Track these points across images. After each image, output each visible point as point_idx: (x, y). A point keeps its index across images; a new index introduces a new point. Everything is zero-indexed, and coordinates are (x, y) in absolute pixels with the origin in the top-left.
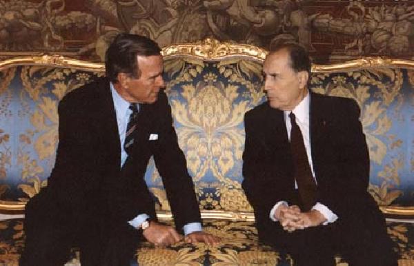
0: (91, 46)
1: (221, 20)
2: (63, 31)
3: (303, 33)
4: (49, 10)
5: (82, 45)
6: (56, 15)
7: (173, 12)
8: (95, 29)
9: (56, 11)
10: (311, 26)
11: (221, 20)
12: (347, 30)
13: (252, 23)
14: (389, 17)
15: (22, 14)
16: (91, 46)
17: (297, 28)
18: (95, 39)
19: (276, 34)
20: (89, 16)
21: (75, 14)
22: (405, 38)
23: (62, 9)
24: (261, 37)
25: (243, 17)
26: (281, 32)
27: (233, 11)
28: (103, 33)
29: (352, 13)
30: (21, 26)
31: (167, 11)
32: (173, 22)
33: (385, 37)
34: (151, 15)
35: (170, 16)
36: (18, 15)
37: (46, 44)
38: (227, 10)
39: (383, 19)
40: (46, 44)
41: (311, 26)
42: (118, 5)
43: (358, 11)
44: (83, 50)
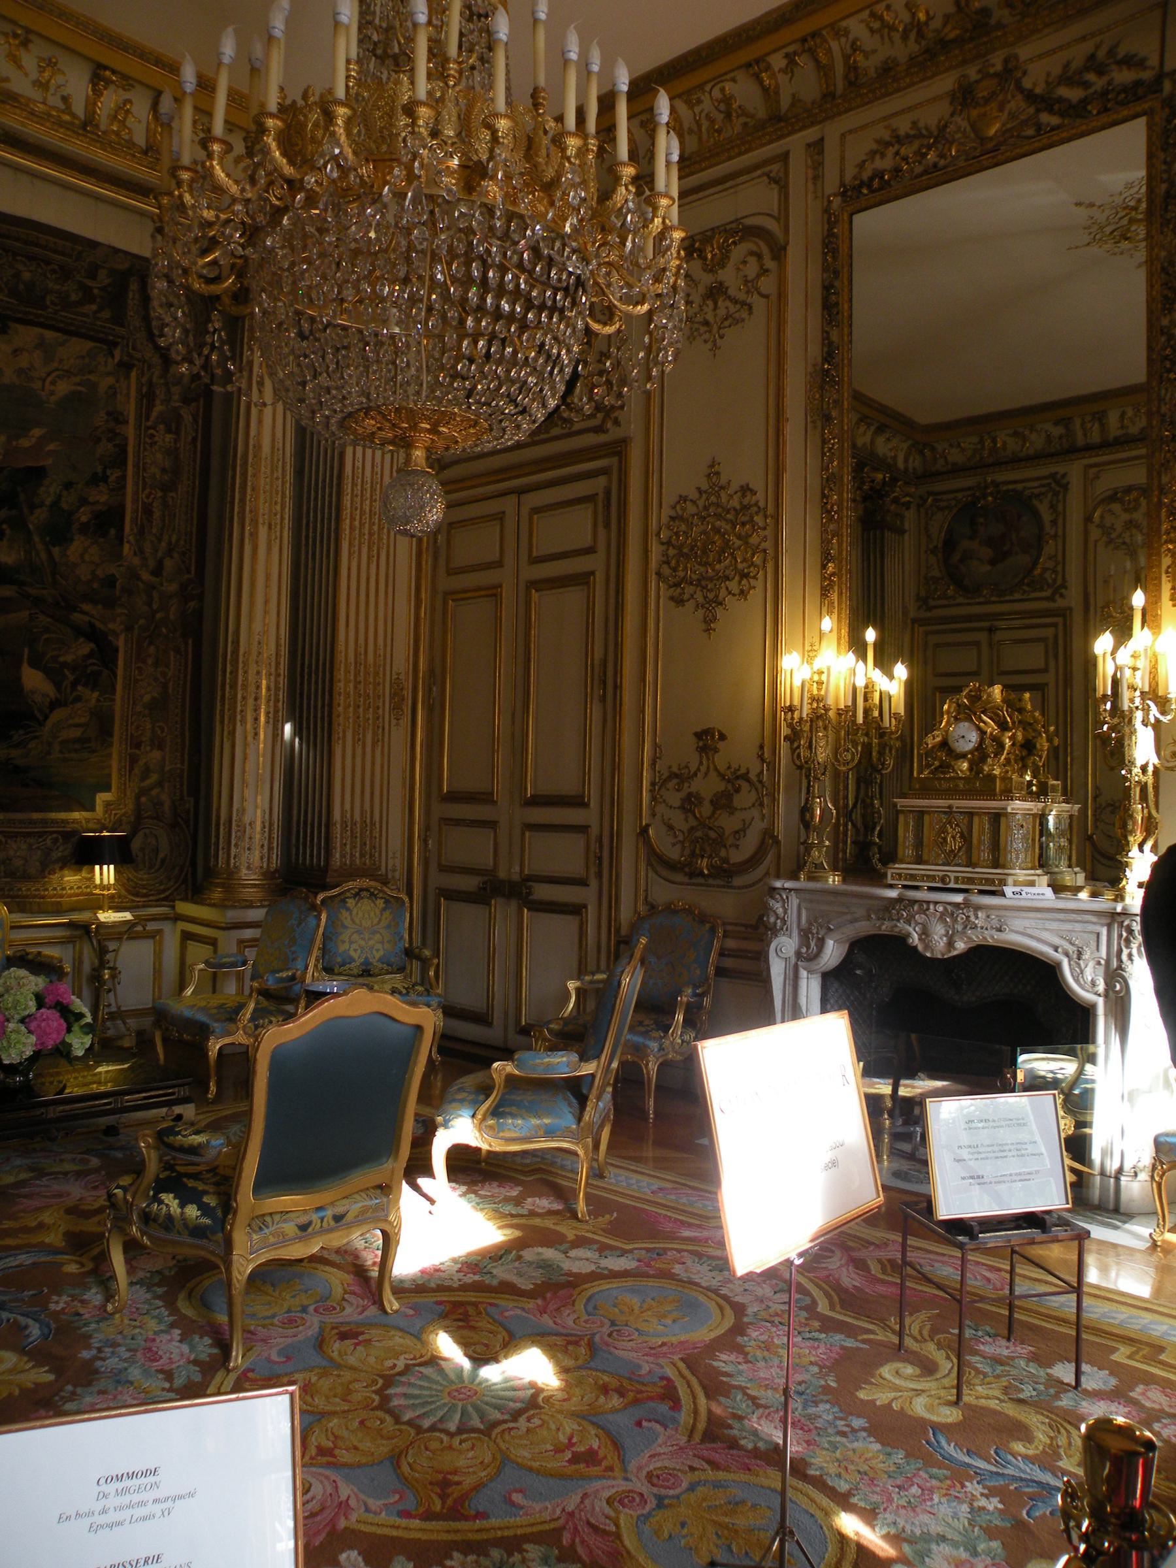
14: (24, 846)
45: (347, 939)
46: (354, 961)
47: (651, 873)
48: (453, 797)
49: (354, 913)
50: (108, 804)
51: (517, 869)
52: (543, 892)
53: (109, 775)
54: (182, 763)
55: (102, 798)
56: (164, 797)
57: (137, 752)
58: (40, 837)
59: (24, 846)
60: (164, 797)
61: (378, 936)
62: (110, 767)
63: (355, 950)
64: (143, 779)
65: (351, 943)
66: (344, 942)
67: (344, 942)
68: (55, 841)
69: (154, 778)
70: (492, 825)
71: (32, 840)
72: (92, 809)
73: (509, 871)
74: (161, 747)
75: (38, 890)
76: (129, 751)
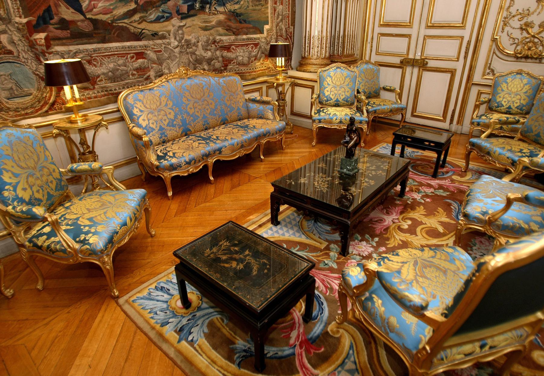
0: (148, 74)
1: (194, 57)
2: (137, 70)
3: (220, 59)
4: (129, 60)
5: (144, 75)
6: (133, 62)
7: (178, 56)
8: (149, 67)
9: (132, 60)
10: (222, 57)
11: (194, 57)
12: (232, 56)
13: (204, 57)
15: (117, 63)
16: (148, 74)
17: (218, 57)
18: (149, 71)
19: (212, 61)
20: (146, 60)
21: (140, 61)
22: (247, 58)
23: (134, 59)
24: (208, 63)
25: (201, 55)
26: (214, 59)
27: (197, 53)
28: (152, 68)
29: (232, 50)
30: (118, 70)
31: (174, 55)
32: (178, 60)
33: (241, 58)
34: (169, 58)
35: (177, 57)
36: (115, 64)
37: (131, 76)
38: (196, 53)
39: (240, 52)
40: (131, 76)
41: (222, 57)
42: (156, 54)
43: (233, 49)
44: (145, 77)
45: (502, 96)
46: (503, 106)
47: (495, 56)
48: (387, 25)
49: (509, 85)
50: (268, 30)
51: (420, 54)
52: (432, 64)
53: (268, 17)
54: (289, 11)
55: (266, 27)
56: (283, 26)
57: (276, 5)
58: (247, 46)
59: (242, 51)
60: (283, 26)
61: (518, 97)
62: (268, 13)
63: (505, 102)
64: (277, 19)
65: (503, 98)
66: (500, 97)
67: (500, 97)
68: (252, 48)
69: (280, 17)
70: (409, 36)
71: (244, 48)
72: (262, 32)
73: (415, 54)
74: (282, 4)
75: (247, 70)
76: (274, 5)
